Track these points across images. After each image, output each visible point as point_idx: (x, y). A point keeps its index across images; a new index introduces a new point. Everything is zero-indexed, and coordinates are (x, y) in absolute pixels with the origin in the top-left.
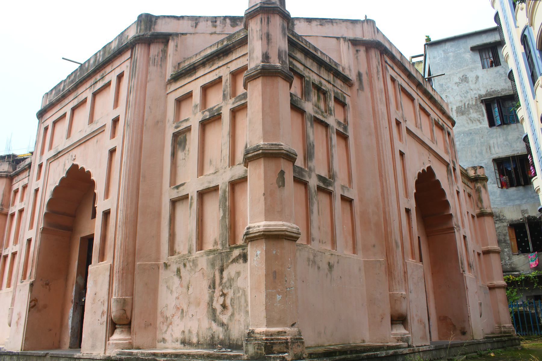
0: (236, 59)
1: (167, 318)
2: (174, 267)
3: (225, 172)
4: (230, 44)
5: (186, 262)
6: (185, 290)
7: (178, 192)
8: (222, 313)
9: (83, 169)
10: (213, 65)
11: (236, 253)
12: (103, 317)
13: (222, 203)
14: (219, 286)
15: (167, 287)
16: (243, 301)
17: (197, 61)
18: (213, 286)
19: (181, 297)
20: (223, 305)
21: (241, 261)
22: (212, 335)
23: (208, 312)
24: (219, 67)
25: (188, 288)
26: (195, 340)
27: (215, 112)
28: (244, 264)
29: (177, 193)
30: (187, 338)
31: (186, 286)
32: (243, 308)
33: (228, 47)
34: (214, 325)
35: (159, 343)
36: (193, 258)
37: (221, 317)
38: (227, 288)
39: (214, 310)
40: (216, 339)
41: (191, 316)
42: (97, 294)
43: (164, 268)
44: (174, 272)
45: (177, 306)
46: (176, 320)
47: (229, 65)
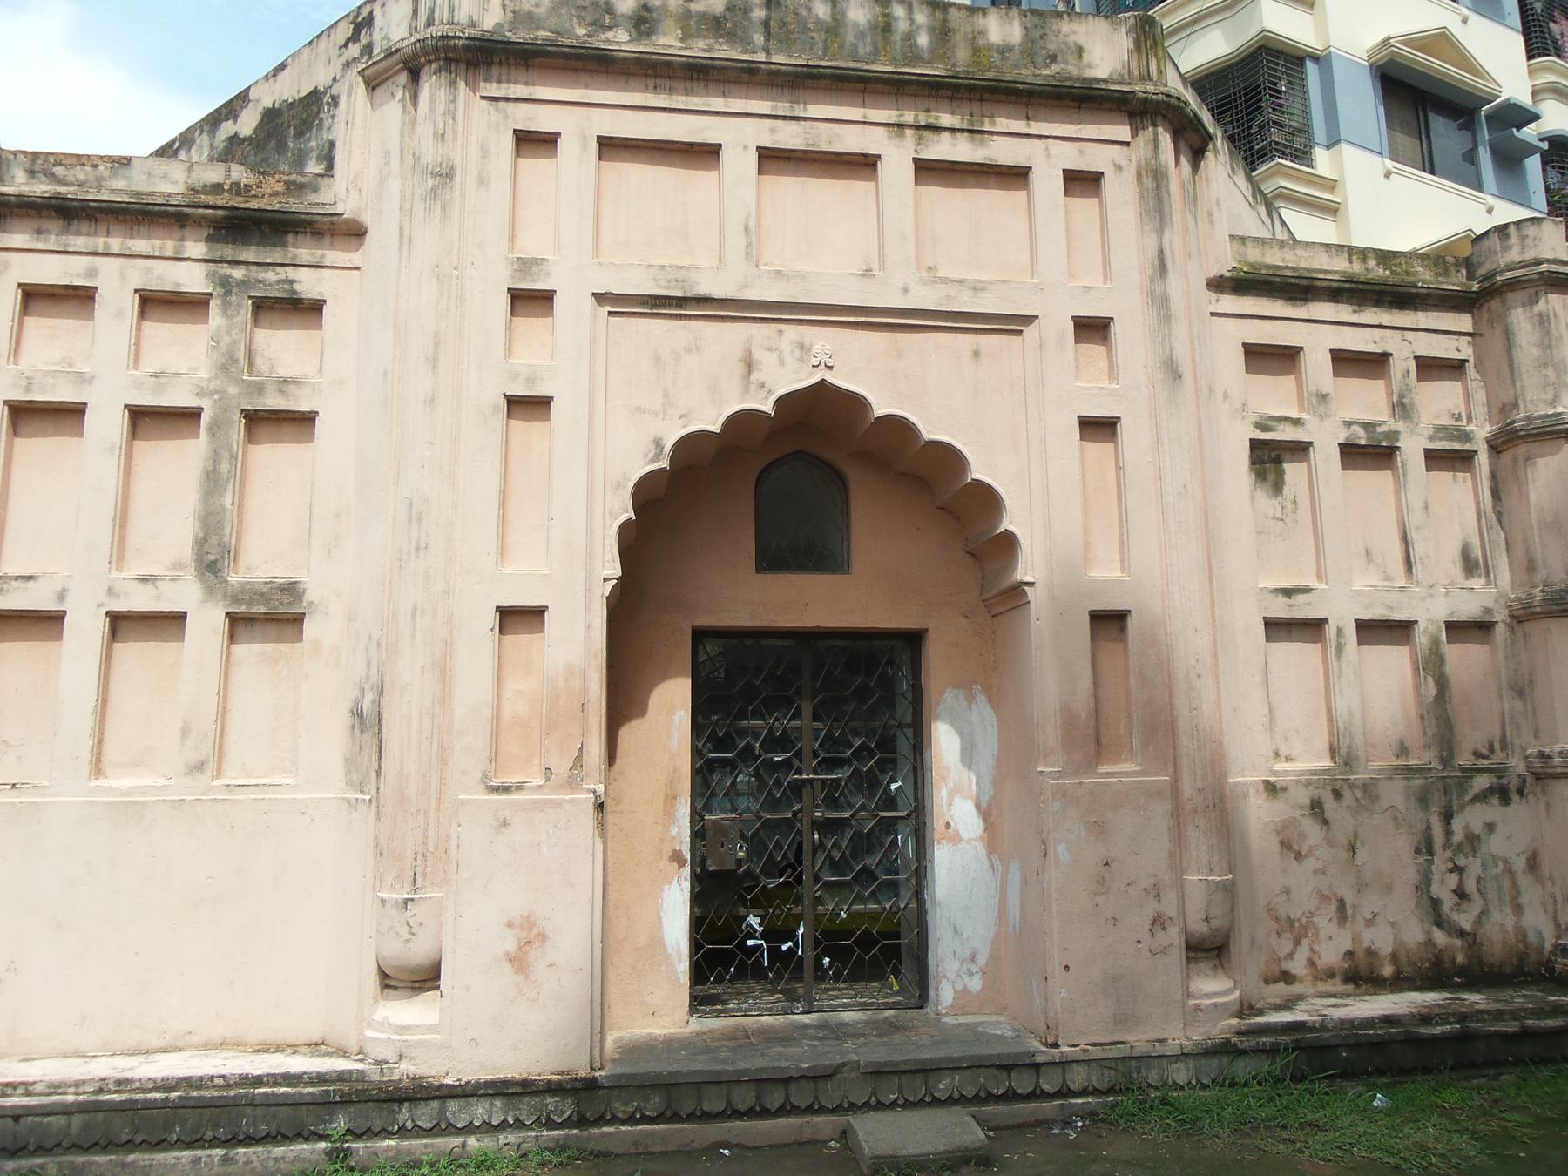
4: (1422, 287)
5: (1341, 787)
6: (1344, 854)
8: (1457, 907)
12: (1160, 934)
14: (1444, 850)
16: (1506, 883)
17: (1321, 276)
18: (1425, 847)
20: (1459, 892)
21: (1495, 801)
22: (1436, 956)
23: (1418, 905)
24: (1380, 326)
25: (1353, 850)
26: (1388, 971)
27: (1382, 437)
28: (1504, 809)
29: (1287, 608)
30: (1363, 967)
31: (1346, 843)
33: (1414, 290)
34: (1440, 938)
35: (1271, 986)
36: (1364, 779)
37: (1455, 916)
39: (1435, 903)
40: (1447, 965)
42: (1114, 866)
44: (1302, 808)
45: (1320, 891)
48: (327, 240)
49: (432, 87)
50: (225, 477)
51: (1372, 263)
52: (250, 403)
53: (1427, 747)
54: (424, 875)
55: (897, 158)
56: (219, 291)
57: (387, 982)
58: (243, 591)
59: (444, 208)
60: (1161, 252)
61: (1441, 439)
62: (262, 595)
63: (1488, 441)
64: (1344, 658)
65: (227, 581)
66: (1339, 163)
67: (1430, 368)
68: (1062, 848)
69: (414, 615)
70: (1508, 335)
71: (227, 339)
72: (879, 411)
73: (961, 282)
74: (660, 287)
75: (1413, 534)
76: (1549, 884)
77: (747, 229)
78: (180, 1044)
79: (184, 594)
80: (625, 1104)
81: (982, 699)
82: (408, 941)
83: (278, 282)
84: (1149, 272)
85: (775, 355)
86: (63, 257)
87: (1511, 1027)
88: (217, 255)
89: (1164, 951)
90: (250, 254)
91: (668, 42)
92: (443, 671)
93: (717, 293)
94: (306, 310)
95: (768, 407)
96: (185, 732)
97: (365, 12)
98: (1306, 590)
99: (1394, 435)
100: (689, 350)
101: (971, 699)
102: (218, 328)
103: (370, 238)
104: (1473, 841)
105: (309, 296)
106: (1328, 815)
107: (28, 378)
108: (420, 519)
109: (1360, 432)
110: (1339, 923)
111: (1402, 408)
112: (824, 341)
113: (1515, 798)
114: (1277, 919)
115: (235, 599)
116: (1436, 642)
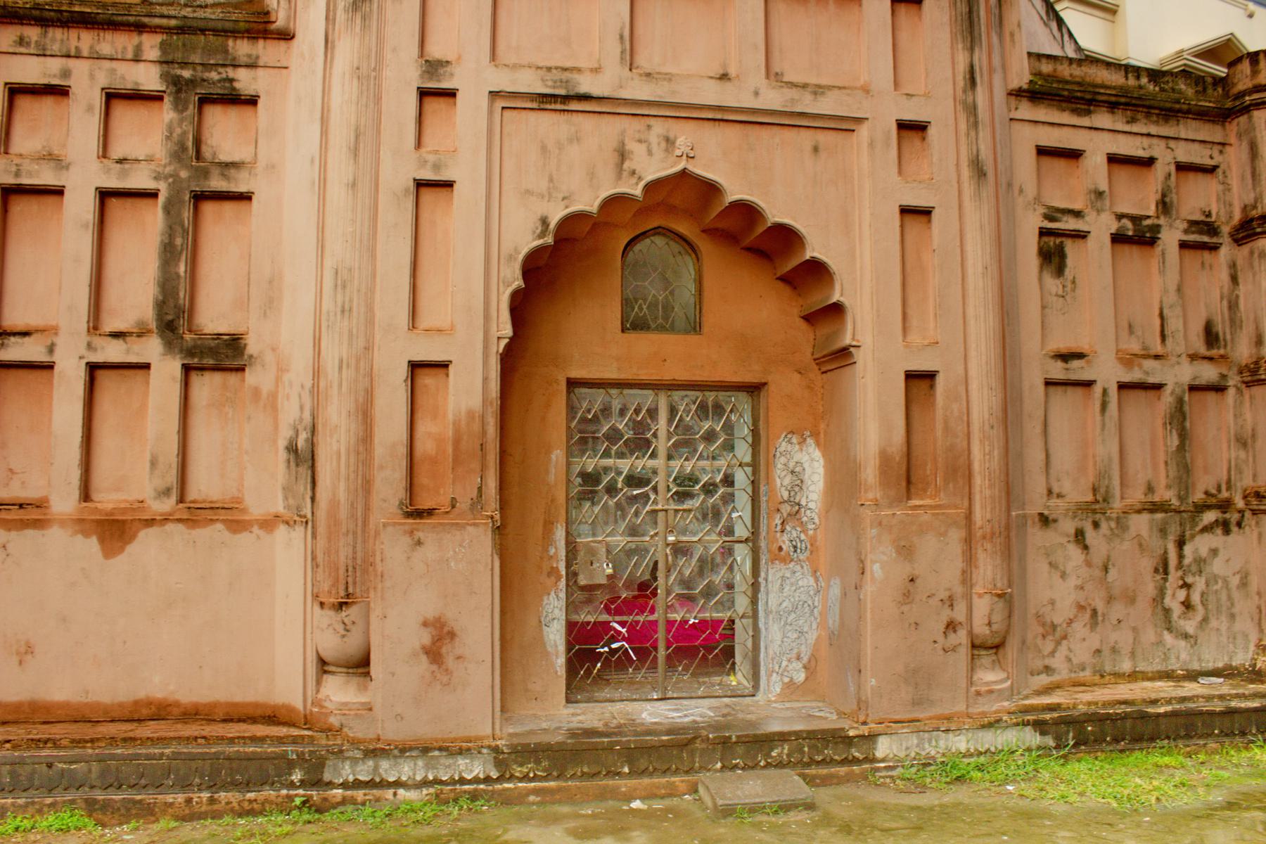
0: (1186, 140)
1: (1054, 627)
2: (1069, 526)
3: (1178, 363)
6: (1098, 573)
7: (1067, 369)
8: (1183, 616)
10: (1132, 120)
11: (1210, 517)
12: (952, 636)
13: (1175, 421)
15: (1050, 564)
16: (1224, 597)
18: (1163, 568)
19: (1088, 587)
21: (1219, 531)
24: (1148, 135)
25: (1106, 569)
27: (1146, 229)
28: (1225, 538)
31: (1100, 564)
32: (1224, 608)
38: (1194, 575)
39: (1167, 611)
41: (1116, 622)
42: (918, 581)
43: (1038, 525)
44: (1068, 536)
46: (1080, 629)
47: (1172, 144)
48: (261, 42)
50: (179, 248)
51: (1144, 80)
52: (198, 185)
53: (1168, 487)
54: (355, 583)
56: (172, 89)
57: (326, 668)
58: (195, 347)
59: (364, 18)
60: (972, 67)
61: (1193, 233)
62: (211, 349)
63: (1231, 235)
64: (1107, 414)
65: (182, 338)
68: (876, 567)
69: (340, 368)
71: (178, 131)
73: (804, 86)
74: (547, 86)
75: (1166, 311)
76: (1256, 598)
77: (621, 37)
78: (163, 713)
79: (151, 349)
80: (521, 765)
81: (810, 441)
82: (343, 636)
83: (219, 81)
84: (961, 83)
85: (643, 147)
86: (42, 59)
87: (1218, 706)
88: (170, 58)
89: (954, 649)
92: (365, 415)
93: (596, 92)
95: (638, 191)
96: (154, 463)
98: (1080, 356)
100: (570, 141)
101: (802, 442)
102: (171, 121)
103: (295, 42)
104: (1200, 562)
105: (246, 93)
106: (1088, 541)
107: (17, 165)
108: (344, 287)
109: (1128, 224)
110: (1091, 627)
112: (685, 136)
113: (1234, 529)
114: (1044, 625)
115: (190, 353)
116: (1180, 401)
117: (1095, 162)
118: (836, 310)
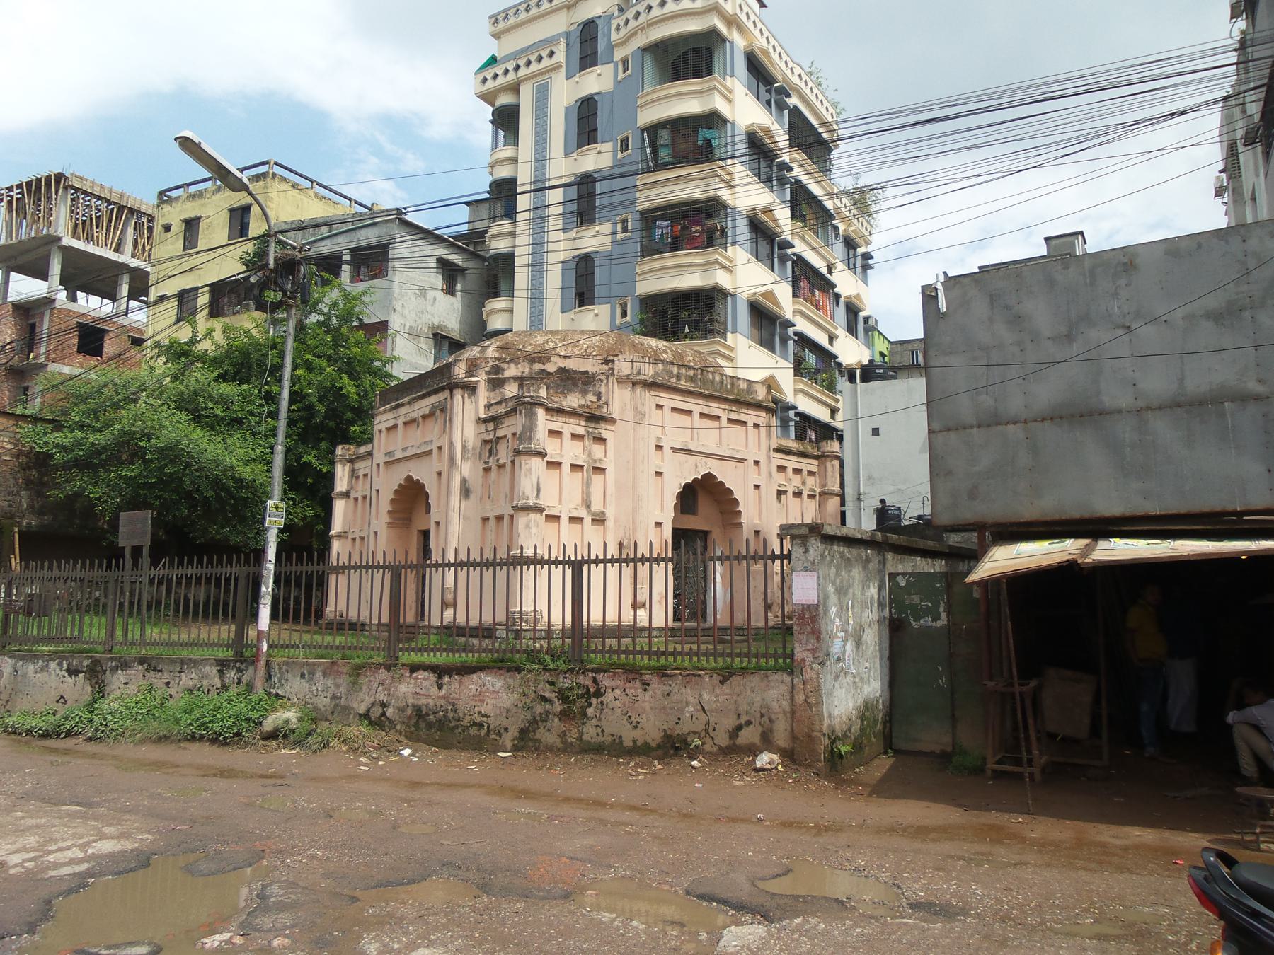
9: (722, 484)
49: (639, 390)
55: (724, 417)
66: (735, 341)
67: (811, 473)
70: (826, 467)
72: (719, 480)
90: (593, 425)
91: (683, 384)
94: (601, 440)
97: (611, 358)
99: (802, 490)
111: (804, 483)
112: (710, 462)
117: (790, 470)
118: (740, 512)
